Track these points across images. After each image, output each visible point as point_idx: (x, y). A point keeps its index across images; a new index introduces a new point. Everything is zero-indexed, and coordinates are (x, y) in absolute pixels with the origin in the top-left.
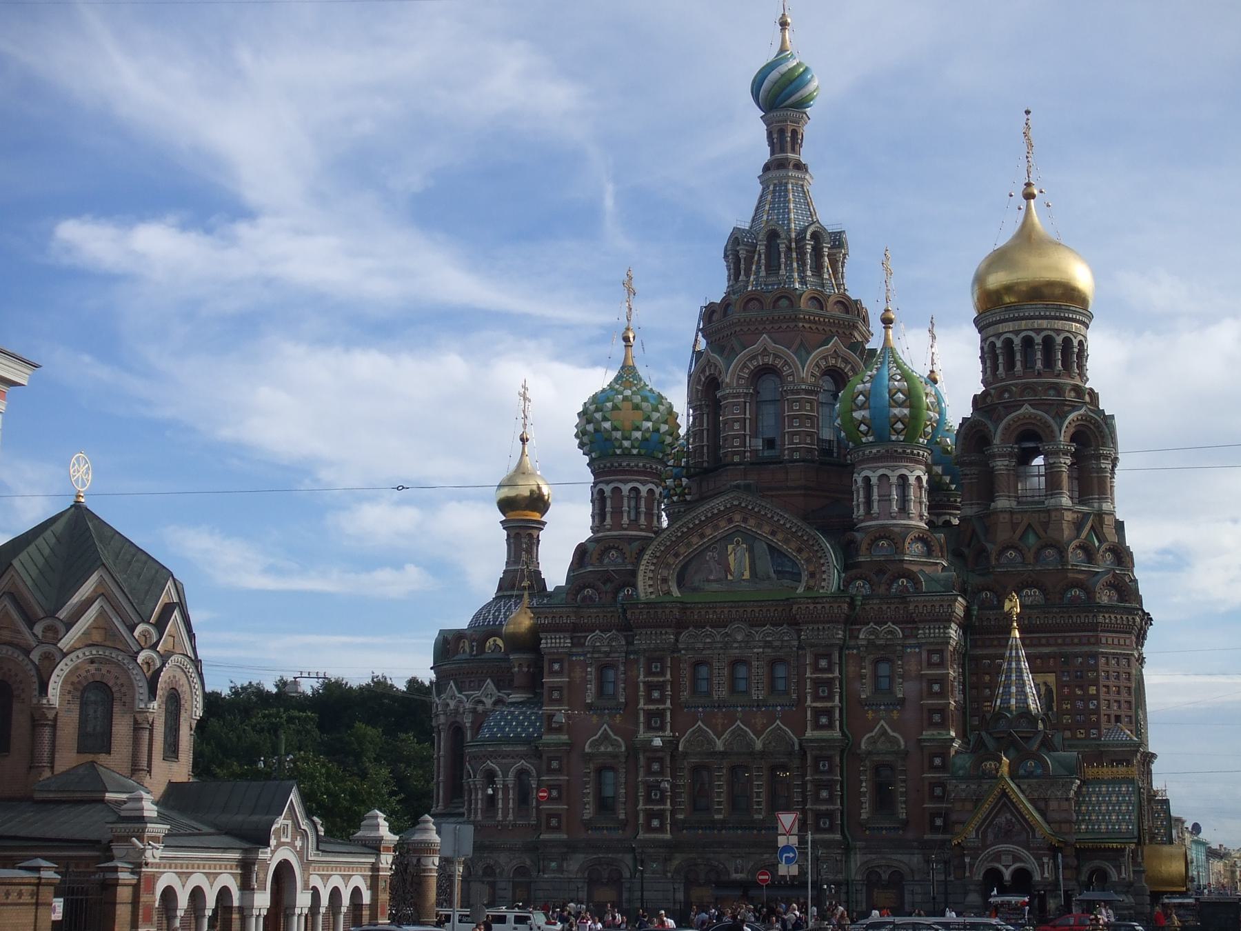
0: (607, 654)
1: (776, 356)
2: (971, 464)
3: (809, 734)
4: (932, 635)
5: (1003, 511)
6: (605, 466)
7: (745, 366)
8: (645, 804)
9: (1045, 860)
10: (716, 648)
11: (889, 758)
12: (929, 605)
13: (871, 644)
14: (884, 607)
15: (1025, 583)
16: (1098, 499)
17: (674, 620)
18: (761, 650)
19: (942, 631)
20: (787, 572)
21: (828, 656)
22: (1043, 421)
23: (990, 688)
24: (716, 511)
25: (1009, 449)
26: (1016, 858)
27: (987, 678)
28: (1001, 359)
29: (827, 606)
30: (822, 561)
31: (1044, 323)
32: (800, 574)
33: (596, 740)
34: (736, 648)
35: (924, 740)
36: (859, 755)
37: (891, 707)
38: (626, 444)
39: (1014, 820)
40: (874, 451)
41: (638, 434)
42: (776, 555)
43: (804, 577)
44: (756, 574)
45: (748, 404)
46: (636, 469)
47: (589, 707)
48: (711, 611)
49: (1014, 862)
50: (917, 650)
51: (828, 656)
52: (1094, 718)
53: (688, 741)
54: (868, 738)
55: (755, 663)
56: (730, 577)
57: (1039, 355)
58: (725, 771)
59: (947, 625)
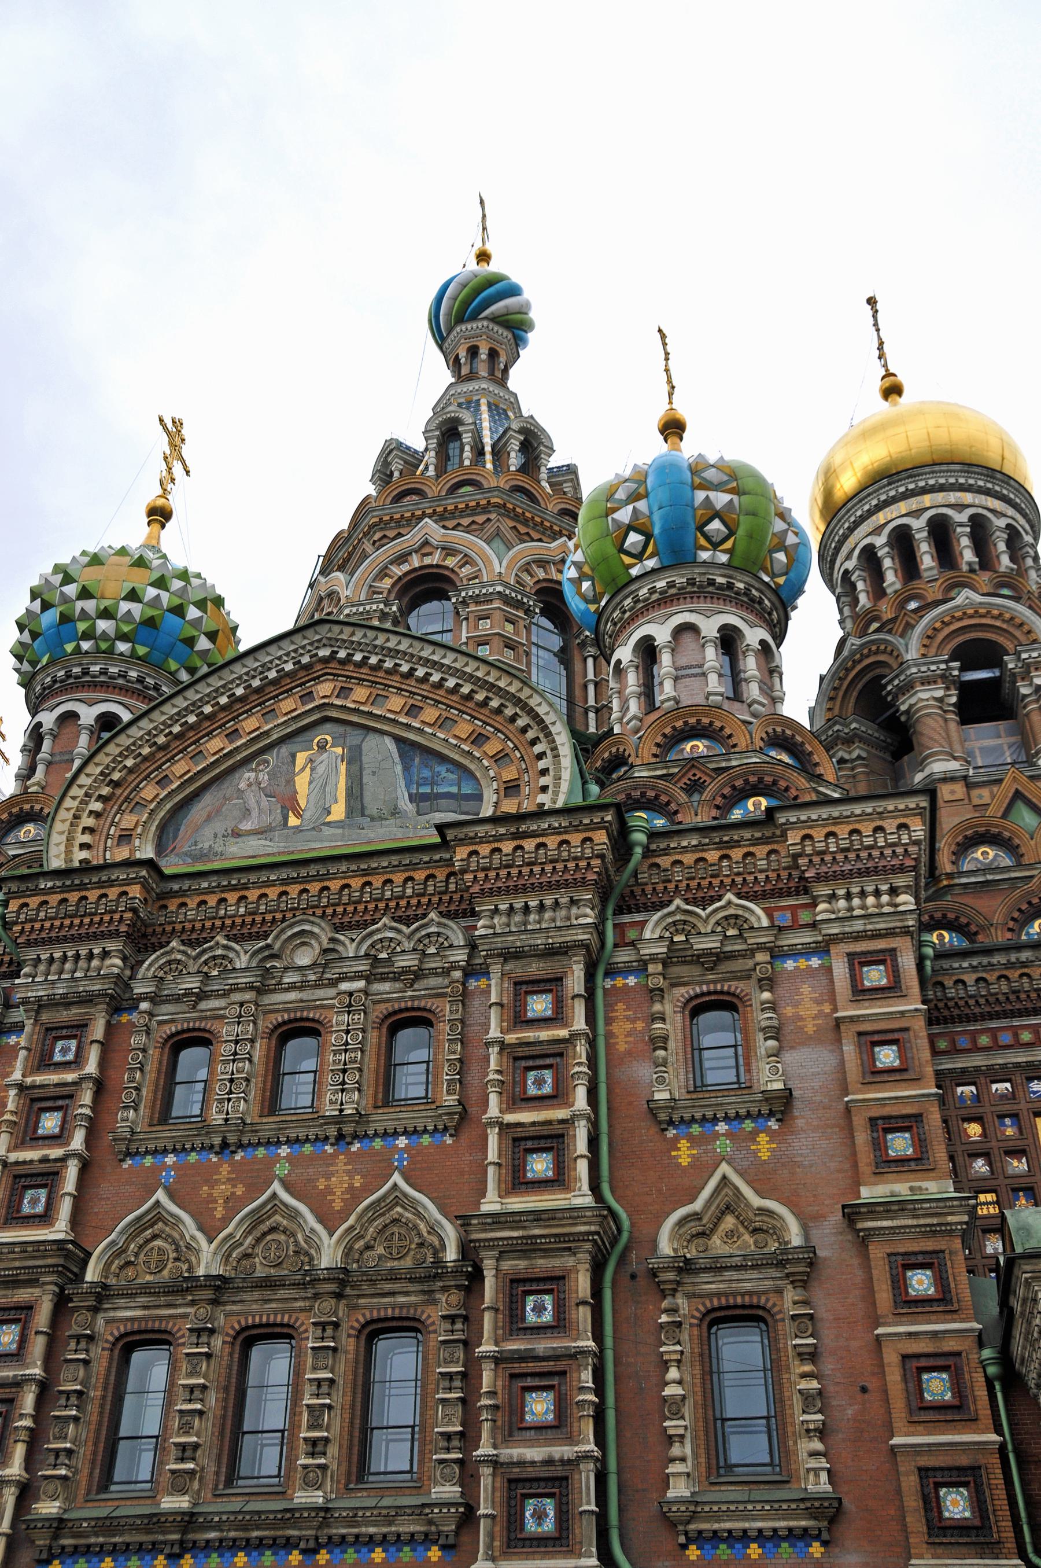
1: (449, 551)
2: (849, 741)
4: (857, 912)
5: (949, 779)
6: (55, 682)
7: (383, 574)
10: (235, 989)
11: (749, 1282)
12: (843, 831)
14: (712, 856)
17: (128, 915)
18: (361, 984)
19: (885, 898)
20: (448, 796)
21: (552, 984)
22: (1007, 616)
23: (986, 1155)
24: (272, 675)
25: (943, 666)
27: (974, 1130)
28: (887, 563)
29: (552, 842)
30: (538, 749)
31: (968, 498)
32: (479, 797)
34: (292, 987)
35: (873, 1209)
36: (653, 1273)
37: (748, 1125)
38: (102, 625)
40: (661, 584)
41: (136, 609)
42: (417, 760)
43: (490, 797)
44: (363, 808)
46: (120, 681)
48: (232, 897)
50: (815, 962)
51: (552, 984)
53: (123, 1251)
54: (682, 1222)
55: (339, 1020)
56: (293, 821)
57: (965, 541)
59: (901, 881)
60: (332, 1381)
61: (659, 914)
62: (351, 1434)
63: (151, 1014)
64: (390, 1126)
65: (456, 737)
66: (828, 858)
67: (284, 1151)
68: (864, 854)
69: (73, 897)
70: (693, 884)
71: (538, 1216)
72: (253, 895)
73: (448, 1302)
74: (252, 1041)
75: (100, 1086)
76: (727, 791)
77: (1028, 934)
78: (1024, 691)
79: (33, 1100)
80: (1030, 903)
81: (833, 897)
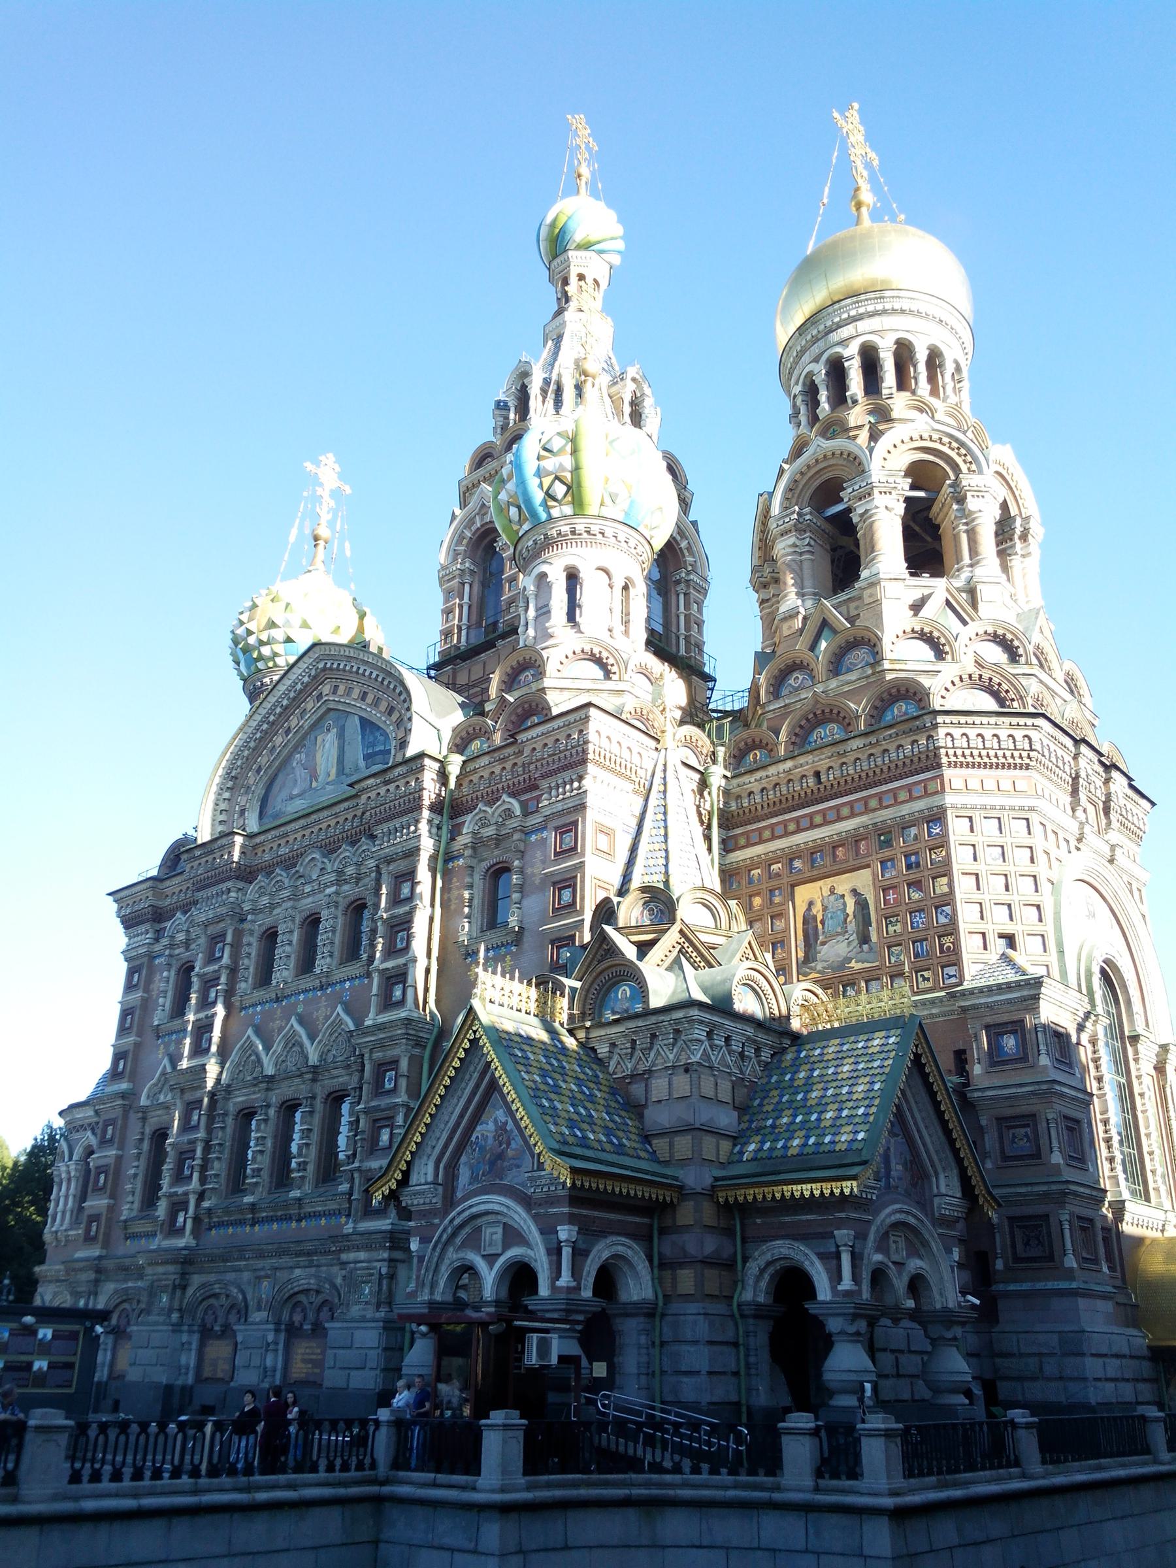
0: (187, 944)
3: (368, 1023)
7: (461, 537)
8: (172, 1185)
9: (565, 1232)
13: (477, 844)
15: (811, 716)
16: (971, 566)
18: (333, 889)
19: (576, 785)
20: (381, 752)
24: (299, 687)
26: (512, 1236)
29: (401, 783)
33: (155, 1085)
39: (510, 1125)
40: (530, 543)
43: (393, 752)
45: (467, 587)
47: (158, 1033)
48: (283, 842)
49: (506, 1246)
50: (545, 834)
52: (948, 942)
53: (238, 1064)
55: (324, 914)
56: (314, 784)
58: (272, 1112)
60: (309, 1130)
61: (470, 816)
62: (320, 1158)
63: (253, 921)
64: (341, 975)
65: (380, 712)
66: (544, 762)
67: (301, 997)
68: (562, 755)
69: (210, 858)
70: (489, 790)
71: (380, 1027)
72: (291, 839)
73: (356, 1077)
74: (291, 932)
75: (233, 970)
76: (513, 718)
77: (810, 743)
78: (855, 520)
79: (206, 982)
80: (808, 720)
81: (551, 788)
